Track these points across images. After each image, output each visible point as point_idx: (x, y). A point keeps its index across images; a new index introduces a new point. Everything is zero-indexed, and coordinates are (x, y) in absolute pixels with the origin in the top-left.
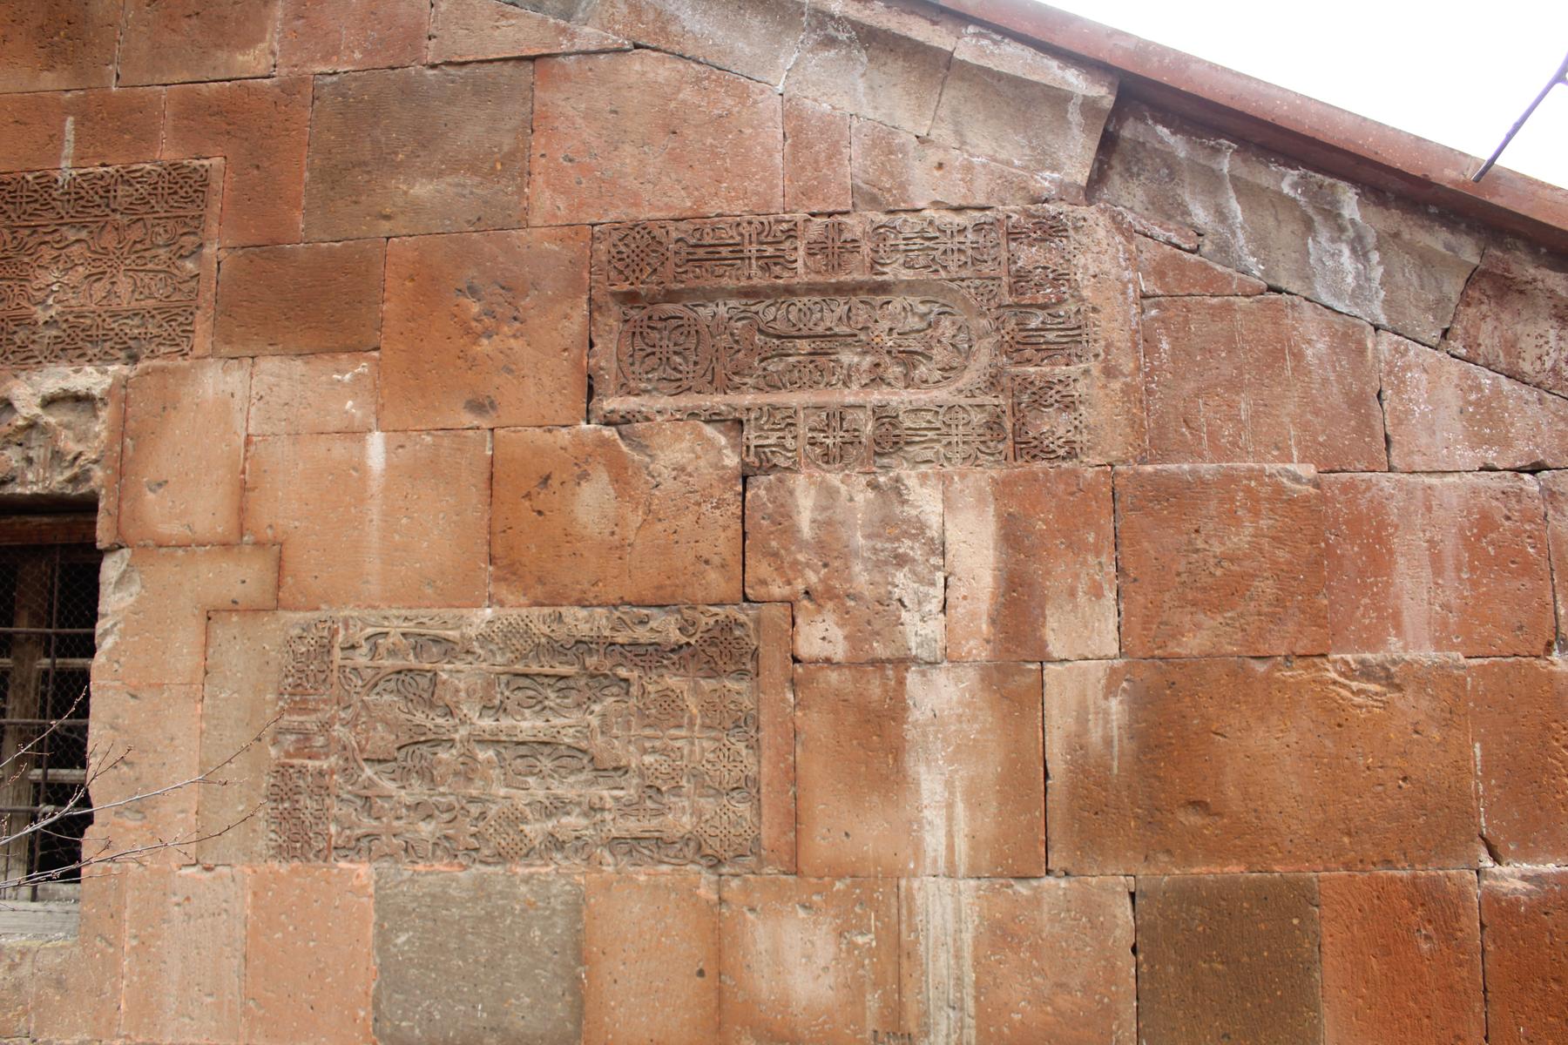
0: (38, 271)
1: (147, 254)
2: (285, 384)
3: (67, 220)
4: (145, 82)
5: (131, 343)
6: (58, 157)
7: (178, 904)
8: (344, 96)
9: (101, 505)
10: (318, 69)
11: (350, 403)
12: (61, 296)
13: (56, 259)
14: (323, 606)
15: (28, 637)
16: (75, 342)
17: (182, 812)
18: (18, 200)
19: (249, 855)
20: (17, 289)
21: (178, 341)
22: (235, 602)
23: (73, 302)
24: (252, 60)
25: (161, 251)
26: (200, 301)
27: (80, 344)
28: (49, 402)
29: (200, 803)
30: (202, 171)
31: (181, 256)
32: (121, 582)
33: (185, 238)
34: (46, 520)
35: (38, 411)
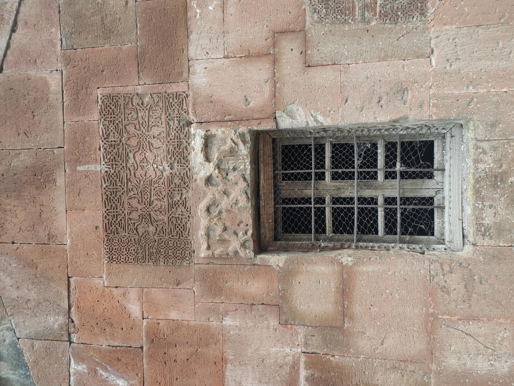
0: (148, 176)
1: (141, 122)
2: (201, 42)
3: (124, 164)
4: (62, 133)
5: (181, 124)
6: (95, 173)
7: (451, 65)
8: (71, 34)
9: (256, 128)
10: (59, 48)
11: (210, 8)
12: (159, 163)
13: (142, 168)
14: (304, 7)
15: (316, 189)
16: (180, 153)
17: (404, 68)
18: (115, 190)
19: (426, 30)
20: (156, 185)
21: (181, 100)
22: (301, 53)
23: (162, 156)
24: (54, 82)
25: (140, 115)
26: (163, 91)
27: (181, 150)
28: (208, 159)
29: (399, 59)
30: (103, 98)
31: (142, 104)
32: (291, 115)
33: (134, 103)
34: (262, 177)
35: (212, 164)
